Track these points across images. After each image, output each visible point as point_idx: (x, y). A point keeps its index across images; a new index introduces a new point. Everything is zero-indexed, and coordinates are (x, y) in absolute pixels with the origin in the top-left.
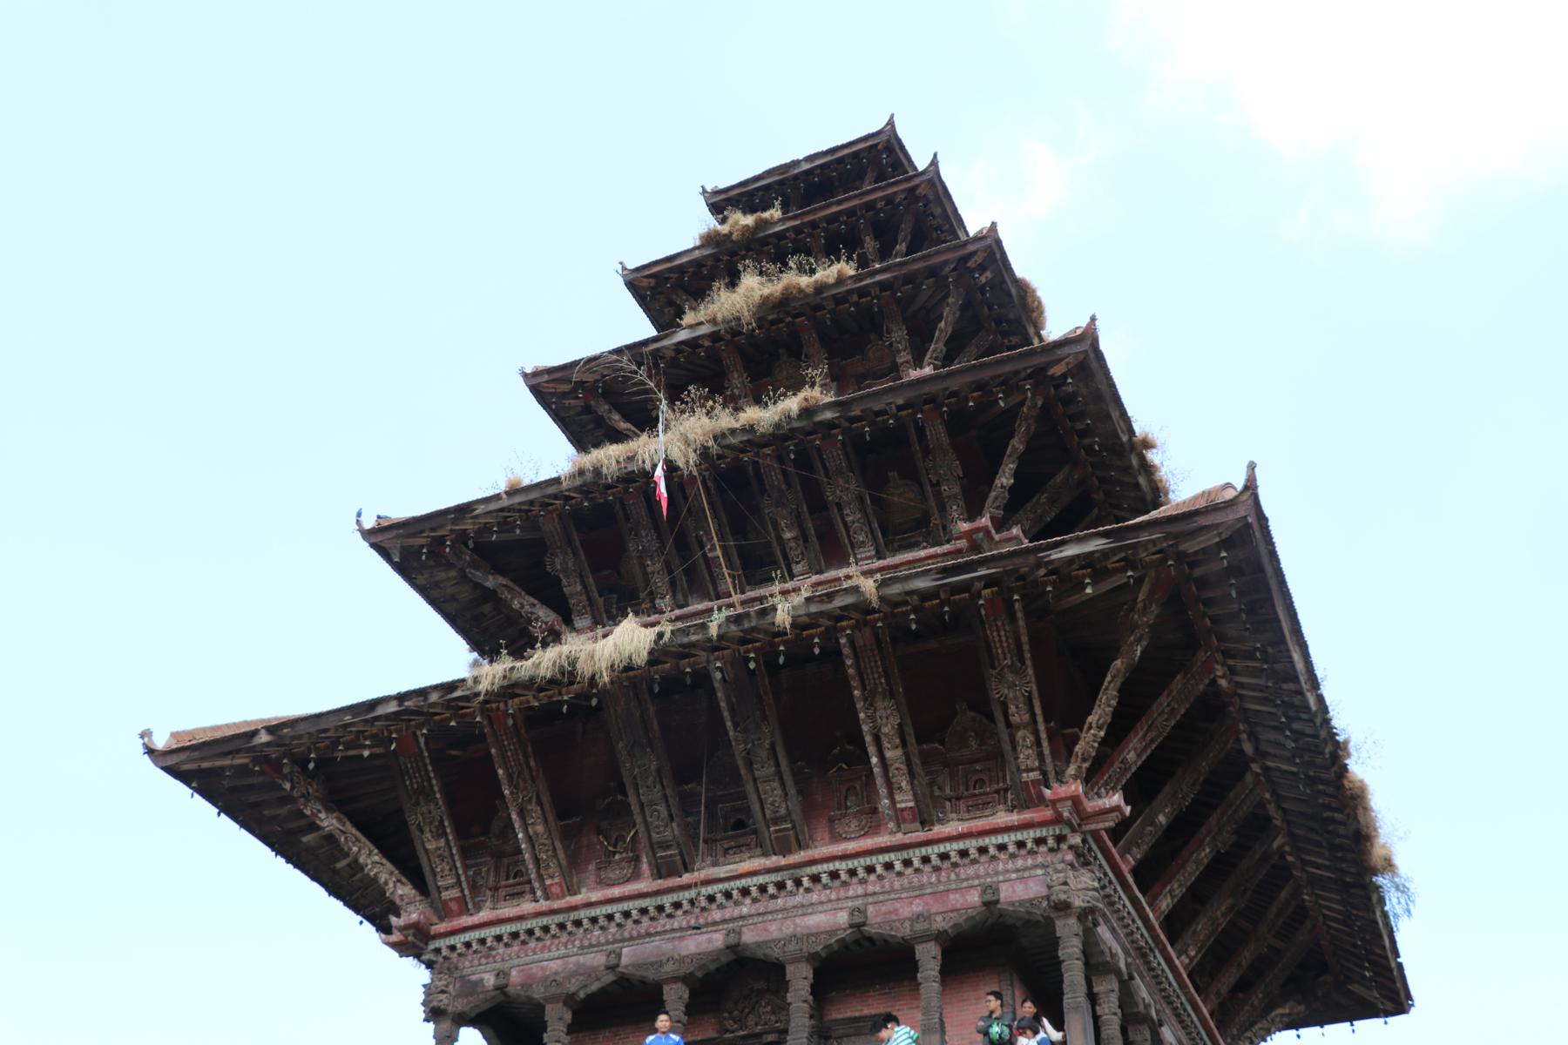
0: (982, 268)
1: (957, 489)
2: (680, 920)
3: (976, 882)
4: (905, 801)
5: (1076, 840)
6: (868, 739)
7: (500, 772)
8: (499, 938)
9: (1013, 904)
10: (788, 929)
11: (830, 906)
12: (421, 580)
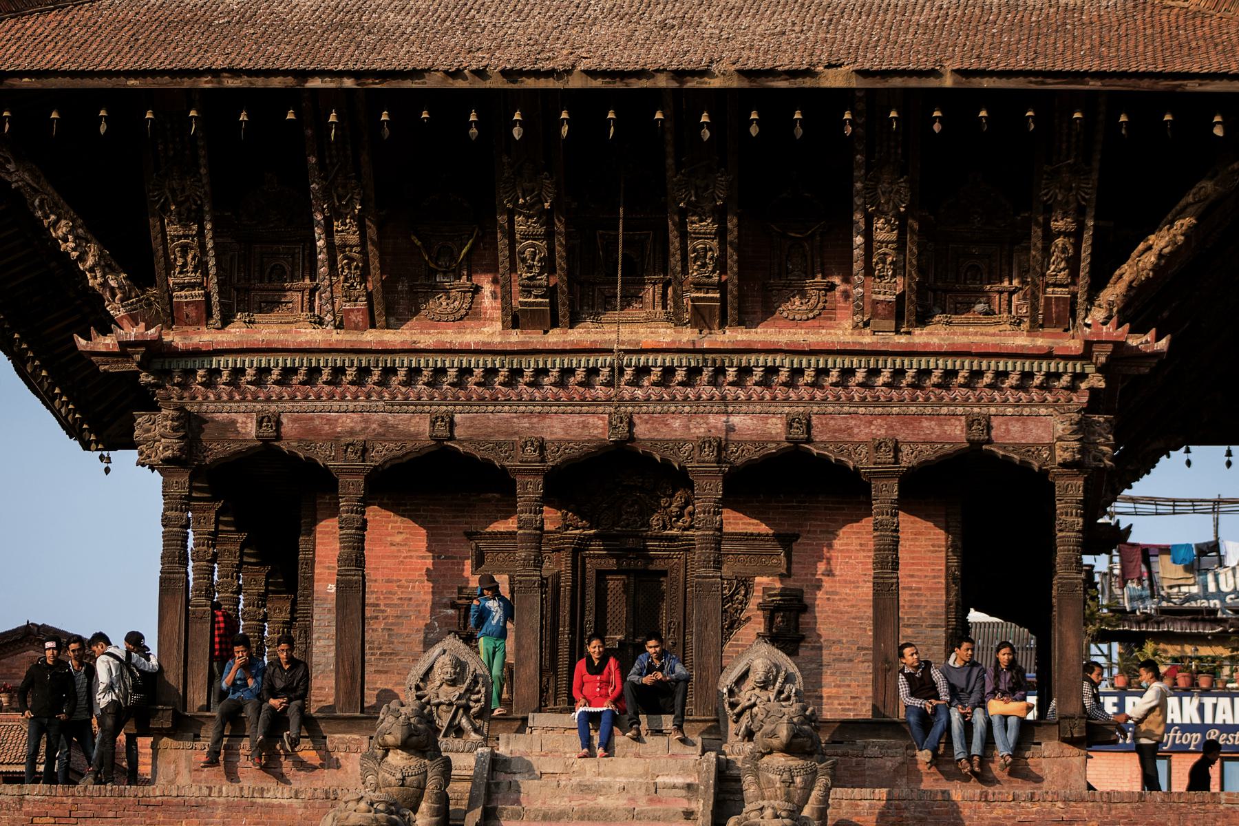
3: (960, 410)
5: (1098, 382)
7: (313, 160)
9: (1004, 447)
11: (758, 408)
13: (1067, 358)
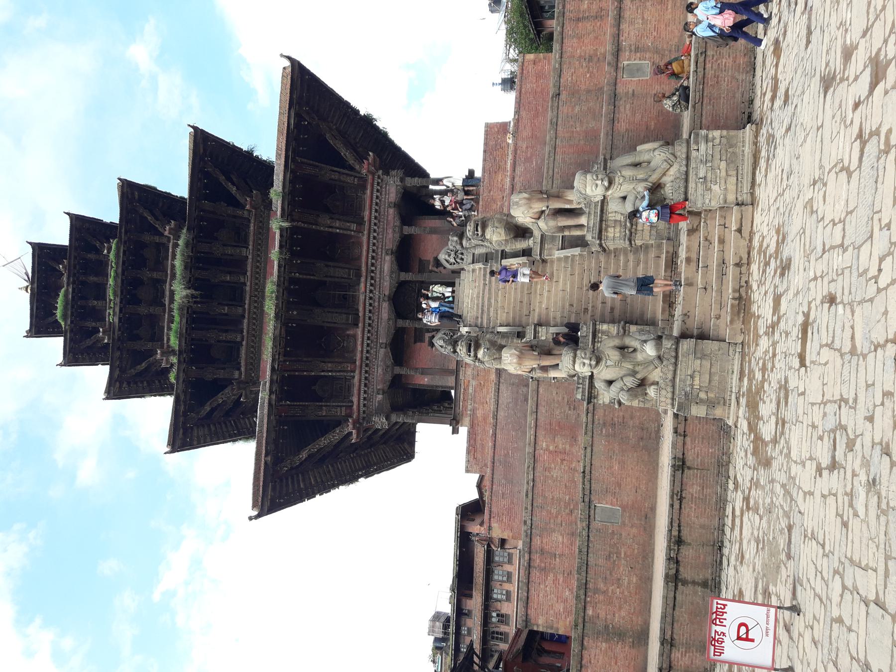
0: (133, 194)
1: (231, 208)
4: (354, 226)
5: (380, 172)
6: (330, 230)
8: (365, 392)
10: (387, 278)
12: (195, 443)
13: (373, 180)
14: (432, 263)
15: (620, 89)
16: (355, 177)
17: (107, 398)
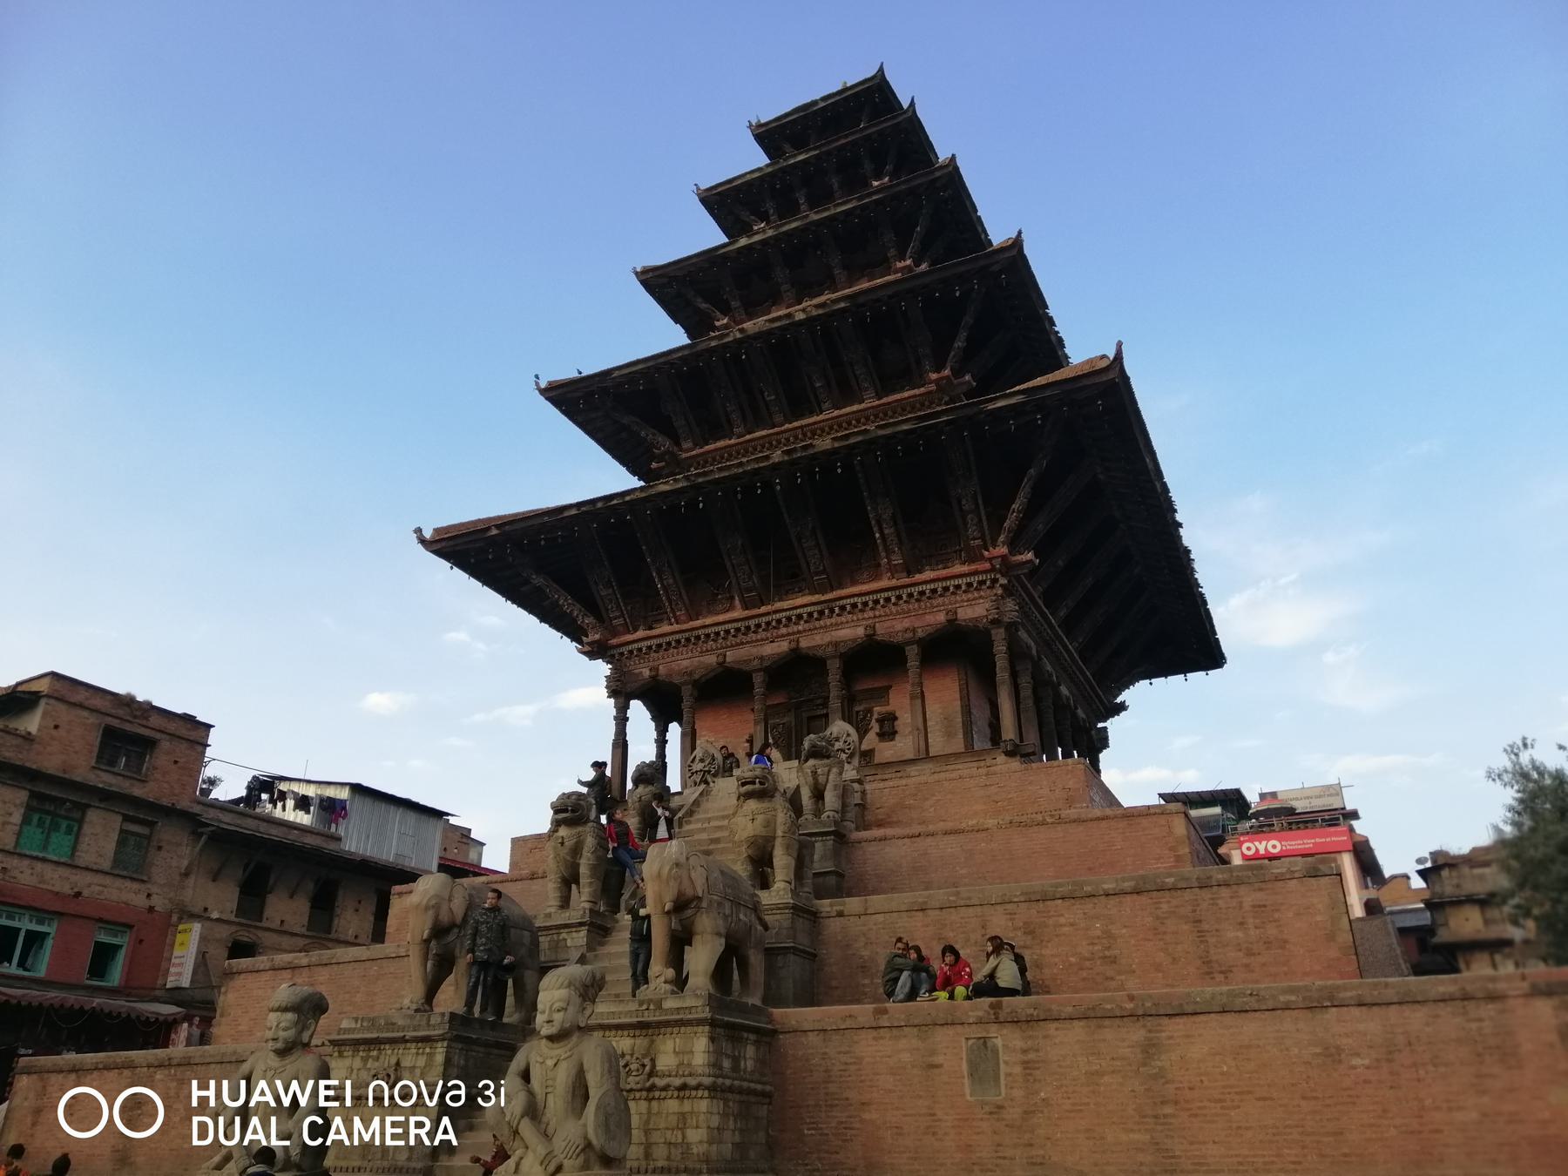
2: (762, 635)
4: (897, 560)
5: (1003, 581)
8: (650, 648)
13: (986, 572)
14: (883, 709)
15: (942, 1036)
16: (983, 538)
17: (636, 273)
